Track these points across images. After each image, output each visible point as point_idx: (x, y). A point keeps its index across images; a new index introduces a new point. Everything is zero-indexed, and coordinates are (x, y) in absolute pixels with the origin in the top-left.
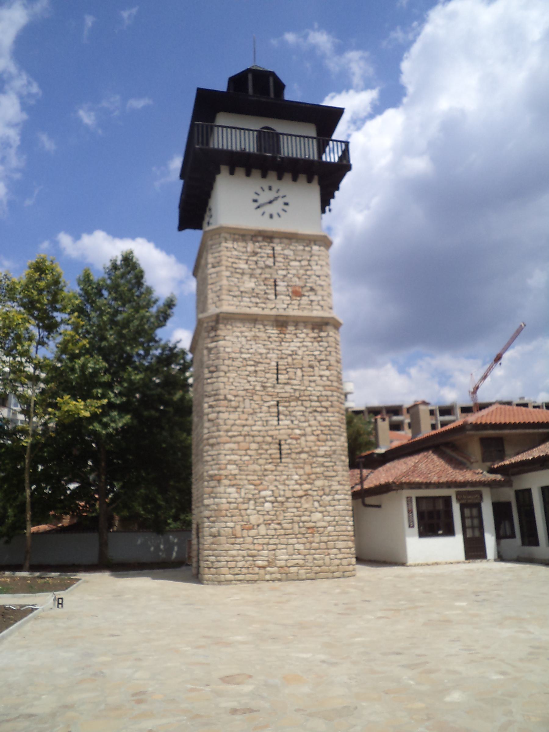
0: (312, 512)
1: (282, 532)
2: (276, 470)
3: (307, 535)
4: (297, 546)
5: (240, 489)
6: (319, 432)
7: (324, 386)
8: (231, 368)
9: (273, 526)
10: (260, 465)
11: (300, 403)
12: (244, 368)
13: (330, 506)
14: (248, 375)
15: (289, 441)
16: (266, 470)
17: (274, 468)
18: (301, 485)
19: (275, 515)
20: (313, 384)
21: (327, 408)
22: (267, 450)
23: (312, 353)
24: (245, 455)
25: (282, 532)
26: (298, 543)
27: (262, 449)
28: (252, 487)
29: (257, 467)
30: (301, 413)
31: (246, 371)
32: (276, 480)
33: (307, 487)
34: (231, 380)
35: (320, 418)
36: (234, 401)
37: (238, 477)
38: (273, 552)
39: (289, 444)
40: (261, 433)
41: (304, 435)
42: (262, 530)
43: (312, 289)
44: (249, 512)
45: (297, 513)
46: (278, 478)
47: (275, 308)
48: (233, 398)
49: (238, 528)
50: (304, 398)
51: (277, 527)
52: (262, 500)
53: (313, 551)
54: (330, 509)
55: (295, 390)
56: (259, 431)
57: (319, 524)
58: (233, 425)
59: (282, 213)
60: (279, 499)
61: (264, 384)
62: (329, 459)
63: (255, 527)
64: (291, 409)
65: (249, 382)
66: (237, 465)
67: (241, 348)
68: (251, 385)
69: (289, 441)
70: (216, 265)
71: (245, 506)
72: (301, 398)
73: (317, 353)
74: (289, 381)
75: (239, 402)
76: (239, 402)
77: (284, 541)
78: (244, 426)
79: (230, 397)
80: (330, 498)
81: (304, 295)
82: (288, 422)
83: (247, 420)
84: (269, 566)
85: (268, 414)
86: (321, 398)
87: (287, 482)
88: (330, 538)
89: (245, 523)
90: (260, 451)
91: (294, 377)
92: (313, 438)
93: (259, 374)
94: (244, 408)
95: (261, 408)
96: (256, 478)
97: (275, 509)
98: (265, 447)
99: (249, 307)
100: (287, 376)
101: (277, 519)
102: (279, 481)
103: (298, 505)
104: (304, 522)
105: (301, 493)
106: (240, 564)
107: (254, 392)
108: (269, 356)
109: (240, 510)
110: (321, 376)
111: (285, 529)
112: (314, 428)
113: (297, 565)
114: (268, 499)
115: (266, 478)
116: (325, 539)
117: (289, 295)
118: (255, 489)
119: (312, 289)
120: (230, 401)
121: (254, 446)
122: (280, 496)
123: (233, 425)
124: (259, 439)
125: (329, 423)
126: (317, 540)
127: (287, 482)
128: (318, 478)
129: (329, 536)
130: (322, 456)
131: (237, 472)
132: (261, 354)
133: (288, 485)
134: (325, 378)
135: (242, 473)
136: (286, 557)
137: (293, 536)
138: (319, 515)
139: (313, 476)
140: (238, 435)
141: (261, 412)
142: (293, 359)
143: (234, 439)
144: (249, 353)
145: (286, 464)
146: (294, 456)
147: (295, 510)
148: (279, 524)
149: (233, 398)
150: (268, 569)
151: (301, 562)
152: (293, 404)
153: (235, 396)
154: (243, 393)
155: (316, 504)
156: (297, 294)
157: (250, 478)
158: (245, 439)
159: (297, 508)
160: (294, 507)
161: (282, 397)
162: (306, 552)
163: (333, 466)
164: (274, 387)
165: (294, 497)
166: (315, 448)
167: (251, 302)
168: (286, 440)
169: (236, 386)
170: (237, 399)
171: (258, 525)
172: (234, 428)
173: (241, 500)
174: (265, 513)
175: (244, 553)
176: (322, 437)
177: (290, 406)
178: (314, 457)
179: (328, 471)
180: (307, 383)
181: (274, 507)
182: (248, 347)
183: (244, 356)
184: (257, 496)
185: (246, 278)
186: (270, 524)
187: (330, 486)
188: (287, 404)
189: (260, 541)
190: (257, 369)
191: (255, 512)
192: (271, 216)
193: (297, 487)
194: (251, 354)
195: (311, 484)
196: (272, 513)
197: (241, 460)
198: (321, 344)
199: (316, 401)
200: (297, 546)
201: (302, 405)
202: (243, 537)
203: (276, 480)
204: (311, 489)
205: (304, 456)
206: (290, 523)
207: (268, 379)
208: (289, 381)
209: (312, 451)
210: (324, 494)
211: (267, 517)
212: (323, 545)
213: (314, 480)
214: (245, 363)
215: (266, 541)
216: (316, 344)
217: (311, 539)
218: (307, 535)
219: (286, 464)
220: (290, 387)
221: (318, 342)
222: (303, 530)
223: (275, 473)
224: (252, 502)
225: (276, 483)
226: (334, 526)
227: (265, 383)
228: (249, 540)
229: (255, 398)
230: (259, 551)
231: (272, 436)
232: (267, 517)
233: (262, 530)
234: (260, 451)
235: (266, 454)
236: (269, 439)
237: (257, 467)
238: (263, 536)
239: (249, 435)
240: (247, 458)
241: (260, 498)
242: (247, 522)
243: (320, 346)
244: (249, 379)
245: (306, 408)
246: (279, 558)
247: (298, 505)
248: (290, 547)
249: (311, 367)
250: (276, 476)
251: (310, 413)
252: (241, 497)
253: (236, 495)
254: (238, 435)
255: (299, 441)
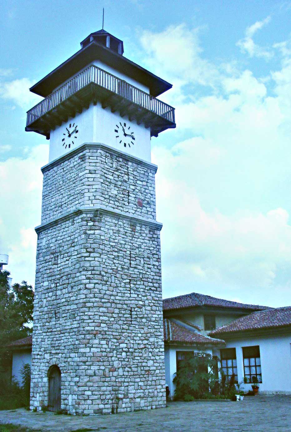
0: (148, 360)
1: (132, 373)
2: (128, 329)
3: (145, 376)
4: (140, 384)
5: (109, 341)
6: (152, 304)
7: (155, 272)
8: (104, 252)
9: (127, 369)
10: (120, 325)
11: (142, 283)
12: (111, 253)
13: (158, 356)
14: (113, 258)
15: (136, 309)
16: (123, 329)
17: (127, 328)
18: (142, 340)
19: (128, 361)
20: (149, 270)
21: (156, 288)
22: (124, 314)
23: (149, 248)
24: (111, 317)
25: (132, 373)
26: (141, 381)
27: (121, 313)
28: (115, 341)
29: (118, 327)
30: (143, 290)
31: (112, 255)
32: (129, 336)
33: (145, 342)
34: (104, 260)
35: (153, 295)
36: (105, 276)
37: (107, 333)
38: (127, 388)
39: (136, 311)
40: (121, 302)
41: (144, 305)
42: (121, 371)
43: (148, 203)
44: (113, 358)
45: (140, 361)
46: (130, 335)
47: (128, 212)
48: (105, 274)
49: (107, 370)
50: (144, 279)
51: (129, 370)
52: (121, 350)
53: (148, 387)
54: (157, 358)
55: (140, 273)
56: (120, 300)
57: (152, 368)
58: (105, 294)
59: (131, 144)
60: (131, 350)
61: (123, 266)
62: (157, 324)
63: (117, 370)
64: (137, 286)
65: (114, 263)
66: (106, 324)
67: (110, 237)
68: (115, 266)
69: (136, 309)
70: (93, 172)
71: (111, 354)
72: (143, 279)
73: (152, 248)
74: (137, 266)
75: (108, 277)
76: (108, 277)
77: (133, 380)
78: (111, 295)
79: (103, 273)
80: (157, 350)
81: (144, 206)
82: (136, 296)
83: (113, 291)
84: (124, 398)
85: (125, 289)
86: (154, 281)
87: (135, 338)
88: (157, 378)
89: (111, 367)
90: (120, 315)
91: (139, 264)
92: (149, 308)
93: (121, 259)
94: (111, 282)
95: (120, 284)
96: (117, 334)
97: (128, 357)
98: (123, 312)
99: (114, 208)
100: (135, 263)
101: (129, 364)
102: (131, 337)
103: (141, 355)
104: (143, 367)
105: (142, 346)
106: (108, 397)
107: (117, 271)
108: (126, 246)
109: (108, 357)
110: (154, 265)
111: (134, 372)
112: (150, 301)
113: (140, 397)
114: (124, 349)
115: (123, 335)
116: (154, 378)
117: (135, 205)
118: (117, 342)
119: (148, 203)
120: (103, 276)
121: (117, 311)
122: (131, 348)
123: (105, 294)
124: (120, 306)
125: (157, 299)
126: (150, 379)
127: (135, 338)
128: (151, 336)
129: (157, 376)
130: (154, 321)
131: (106, 329)
132: (121, 244)
133: (136, 340)
134: (156, 267)
135: (109, 330)
136: (134, 391)
137: (138, 376)
138: (151, 362)
139: (149, 335)
140: (107, 302)
141: (121, 287)
142: (139, 251)
143: (105, 305)
144: (114, 242)
145: (134, 325)
146: (138, 320)
147: (139, 358)
148: (130, 368)
149: (105, 274)
150: (124, 400)
151: (142, 395)
152: (138, 283)
153: (106, 273)
154: (110, 271)
155: (150, 354)
156: (140, 204)
157: (114, 334)
158: (111, 305)
159: (140, 356)
160: (138, 356)
161: (132, 277)
162: (144, 387)
163: (159, 328)
164: (128, 269)
165: (139, 349)
166: (150, 315)
167: (114, 204)
168: (134, 308)
169: (106, 265)
170: (107, 275)
171: (118, 368)
172: (106, 297)
173: (108, 350)
174: (122, 359)
175: (110, 388)
176: (154, 308)
177: (137, 284)
178: (150, 321)
179: (156, 332)
180: (146, 269)
181: (127, 355)
182: (114, 237)
183: (111, 244)
184: (118, 347)
185: (112, 186)
186: (125, 368)
187: (157, 342)
188: (135, 283)
189: (120, 380)
190: (119, 254)
191: (117, 359)
192: (125, 145)
193: (140, 342)
194: (116, 243)
195: (148, 340)
196: (127, 360)
197: (109, 320)
198: (154, 242)
199: (151, 282)
200: (140, 384)
201: (143, 284)
202: (110, 377)
203: (129, 336)
204: (147, 344)
205: (144, 320)
206: (136, 367)
207: (125, 263)
208: (137, 266)
209: (149, 317)
210: (155, 348)
211: (124, 363)
212: (153, 383)
213: (149, 337)
214: (112, 249)
215: (123, 379)
216: (151, 242)
217: (147, 378)
218: (145, 376)
219: (134, 325)
220: (137, 270)
221: (153, 241)
222: (143, 372)
223: (129, 331)
224: (115, 352)
225: (129, 338)
226: (160, 370)
227: (123, 265)
228: (113, 379)
229: (118, 275)
230: (119, 387)
231: (127, 304)
232: (124, 363)
233: (121, 371)
234: (120, 315)
235: (123, 317)
236: (125, 306)
237: (118, 327)
238: (121, 376)
239: (114, 303)
240: (112, 319)
241: (120, 349)
242: (112, 366)
243: (153, 244)
244: (115, 261)
245: (146, 286)
246: (130, 392)
247: (141, 355)
248: (136, 384)
249: (148, 258)
250: (129, 333)
251: (148, 290)
252: (108, 348)
253: (106, 346)
254: (107, 302)
255: (141, 310)
